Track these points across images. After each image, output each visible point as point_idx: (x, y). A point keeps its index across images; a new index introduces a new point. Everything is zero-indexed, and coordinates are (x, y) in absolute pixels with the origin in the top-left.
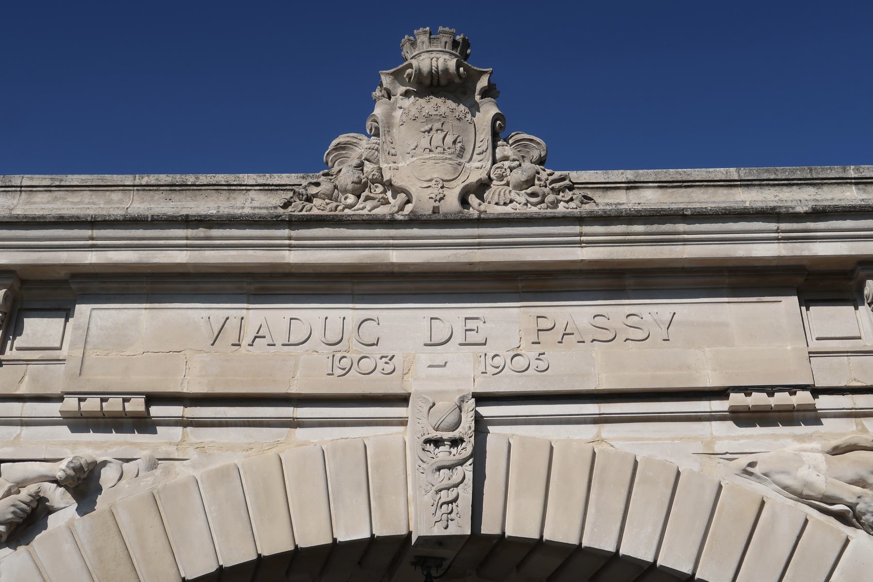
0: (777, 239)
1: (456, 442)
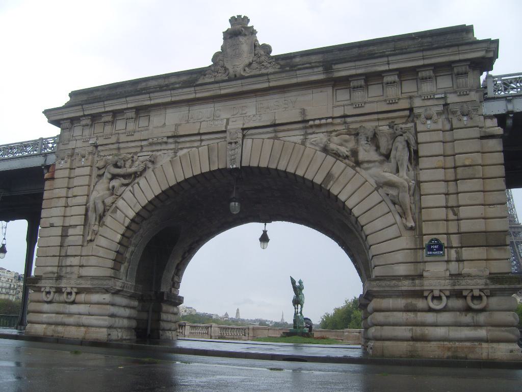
1: (236, 143)
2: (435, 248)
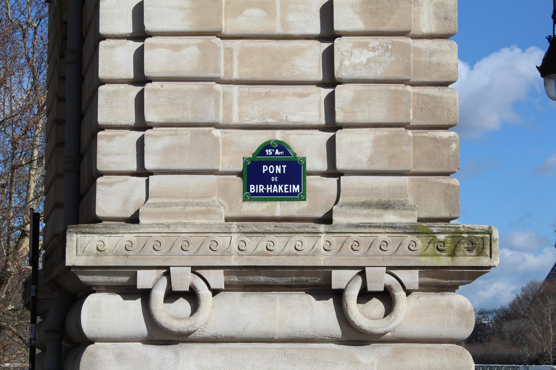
2: (275, 174)
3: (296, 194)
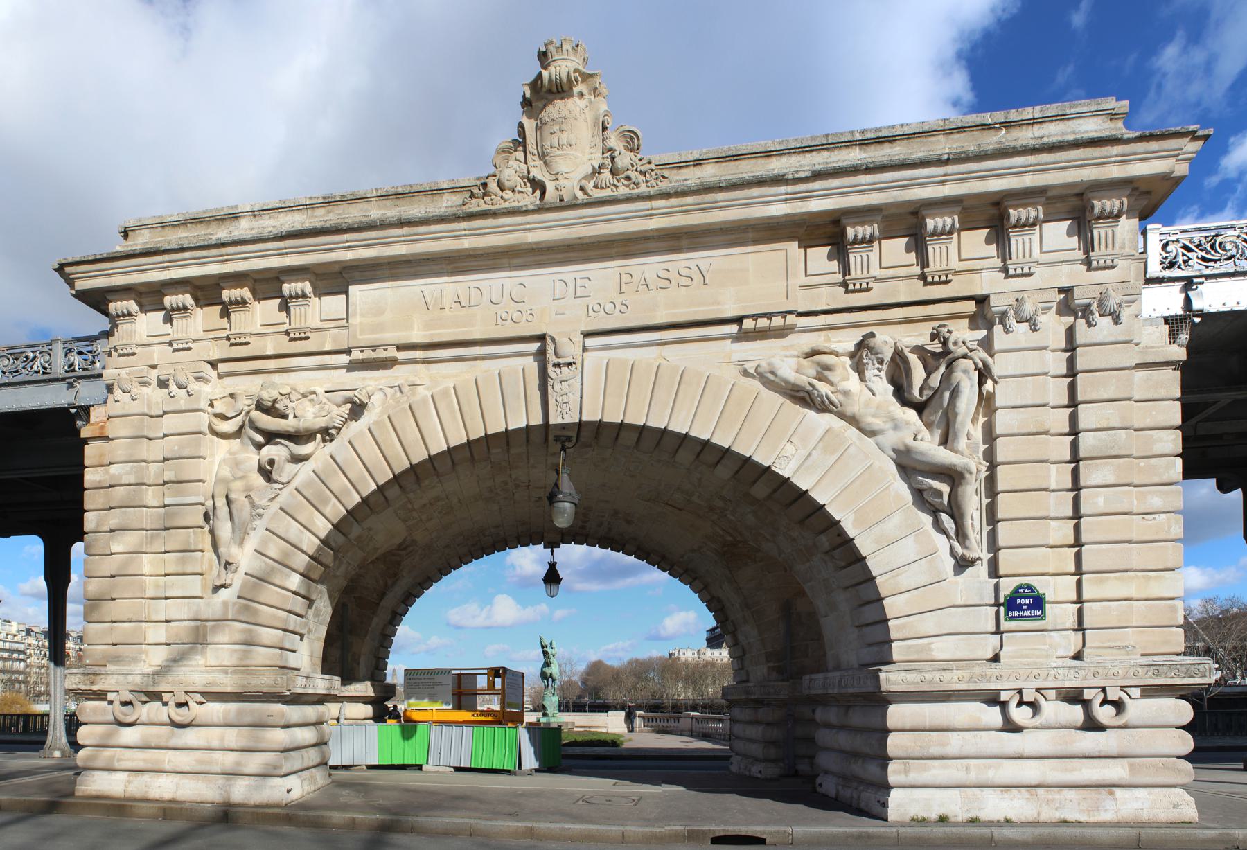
0: (786, 200)
2: (1025, 605)
3: (1039, 616)
